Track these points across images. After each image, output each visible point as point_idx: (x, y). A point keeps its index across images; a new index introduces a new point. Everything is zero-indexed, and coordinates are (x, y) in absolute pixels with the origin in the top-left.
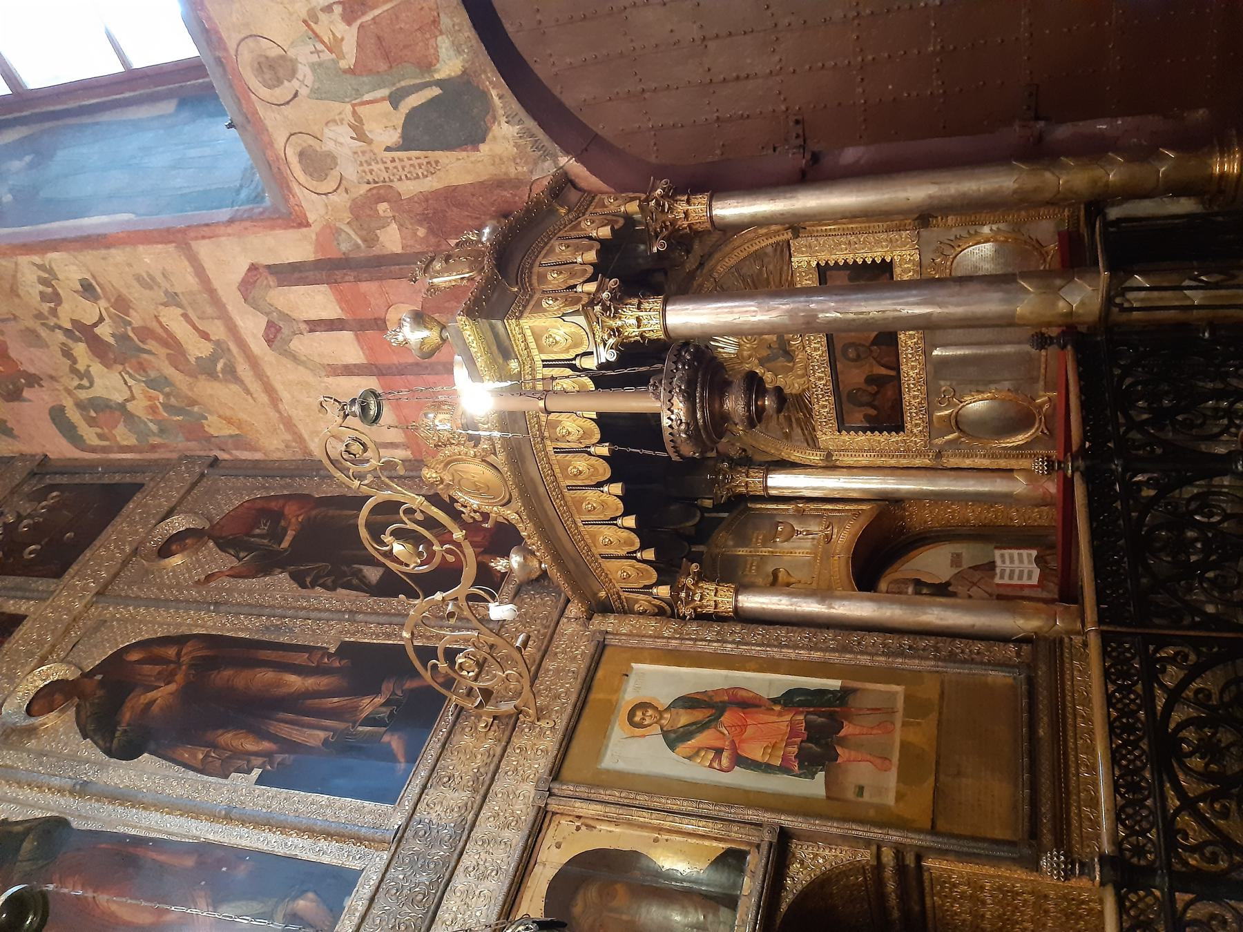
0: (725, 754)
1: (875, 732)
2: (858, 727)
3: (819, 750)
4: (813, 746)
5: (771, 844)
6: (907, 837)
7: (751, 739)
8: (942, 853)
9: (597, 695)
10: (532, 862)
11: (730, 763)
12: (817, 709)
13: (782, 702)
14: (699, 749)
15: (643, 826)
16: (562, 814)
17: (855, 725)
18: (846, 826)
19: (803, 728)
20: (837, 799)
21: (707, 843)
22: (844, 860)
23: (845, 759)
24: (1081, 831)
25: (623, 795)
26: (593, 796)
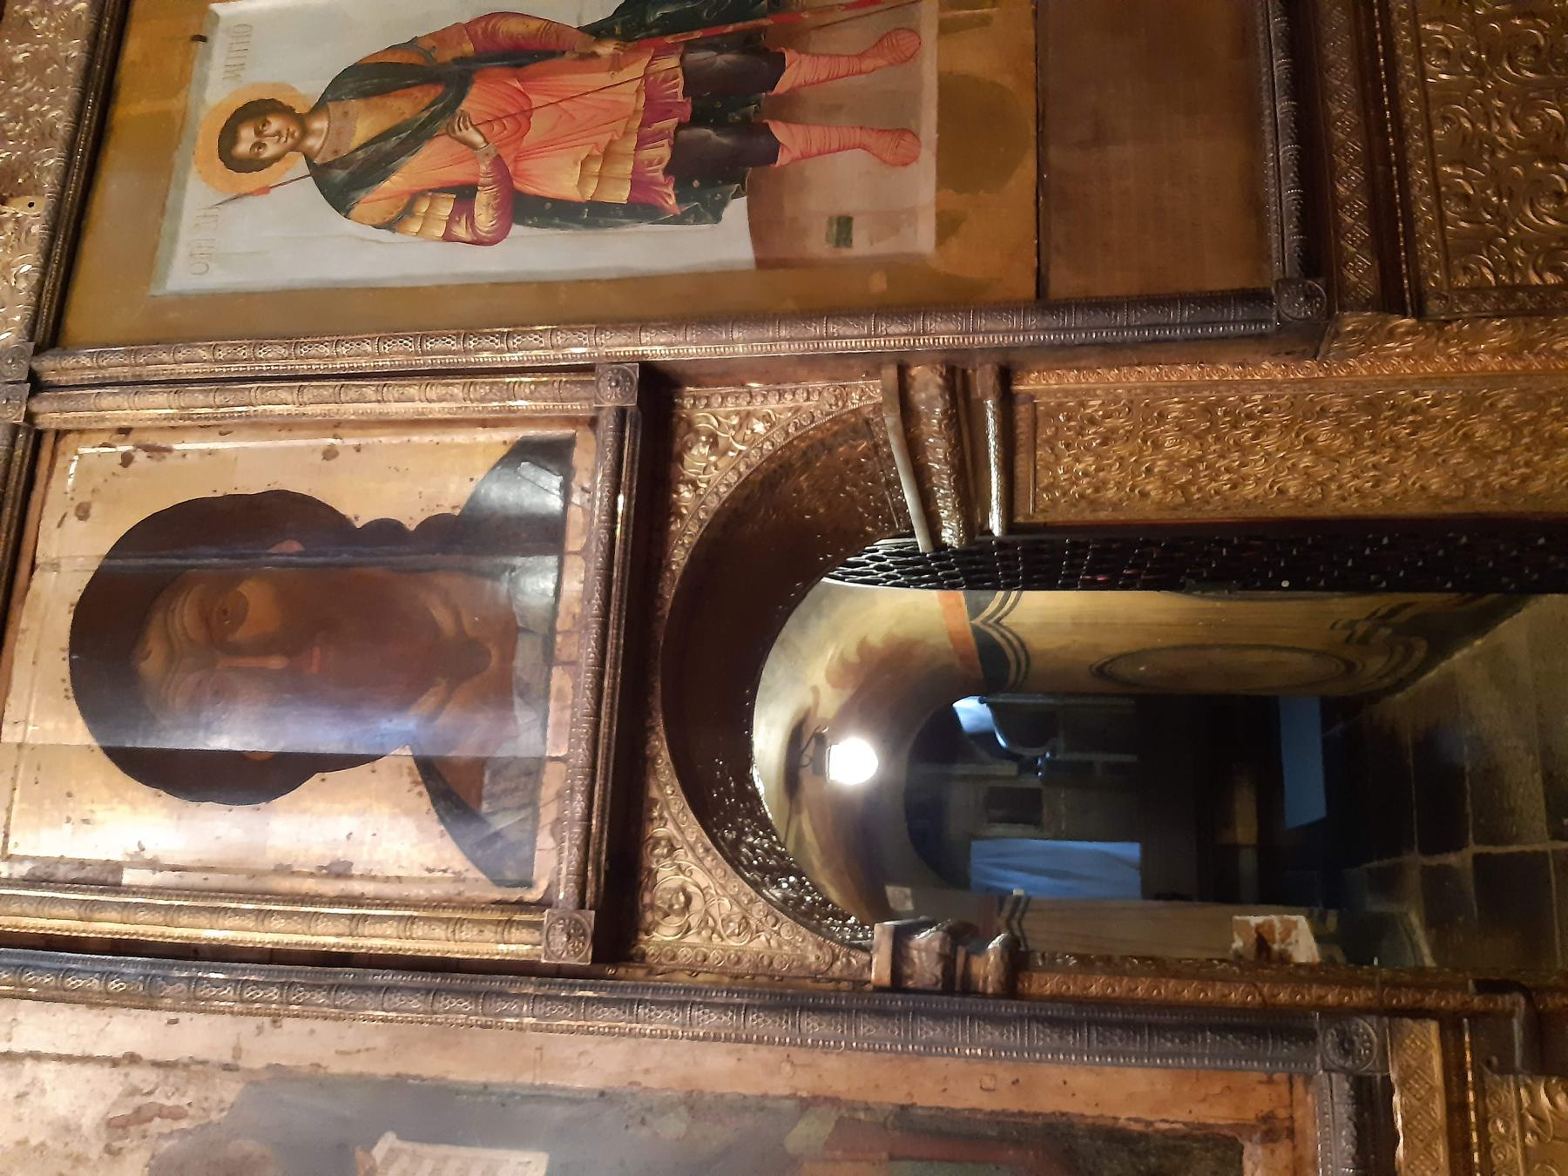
0: (482, 197)
1: (868, 64)
2: (824, 60)
3: (725, 141)
4: (709, 131)
5: (622, 412)
6: (975, 332)
7: (549, 144)
8: (1062, 355)
9: (131, 109)
10: (24, 567)
11: (499, 218)
12: (713, 31)
13: (618, 30)
14: (415, 197)
15: (289, 425)
16: (81, 432)
17: (813, 55)
18: (815, 330)
19: (680, 90)
20: (784, 264)
21: (461, 437)
22: (817, 414)
23: (797, 154)
24: (1443, 231)
25: (221, 355)
26: (149, 371)
